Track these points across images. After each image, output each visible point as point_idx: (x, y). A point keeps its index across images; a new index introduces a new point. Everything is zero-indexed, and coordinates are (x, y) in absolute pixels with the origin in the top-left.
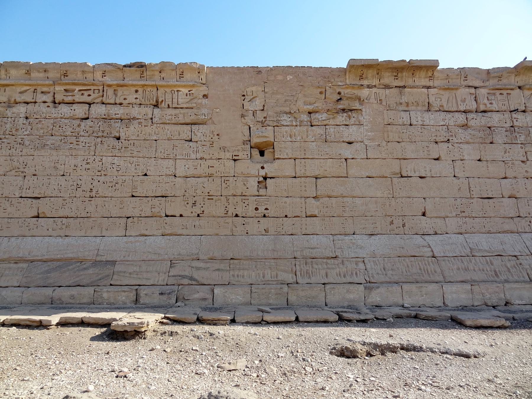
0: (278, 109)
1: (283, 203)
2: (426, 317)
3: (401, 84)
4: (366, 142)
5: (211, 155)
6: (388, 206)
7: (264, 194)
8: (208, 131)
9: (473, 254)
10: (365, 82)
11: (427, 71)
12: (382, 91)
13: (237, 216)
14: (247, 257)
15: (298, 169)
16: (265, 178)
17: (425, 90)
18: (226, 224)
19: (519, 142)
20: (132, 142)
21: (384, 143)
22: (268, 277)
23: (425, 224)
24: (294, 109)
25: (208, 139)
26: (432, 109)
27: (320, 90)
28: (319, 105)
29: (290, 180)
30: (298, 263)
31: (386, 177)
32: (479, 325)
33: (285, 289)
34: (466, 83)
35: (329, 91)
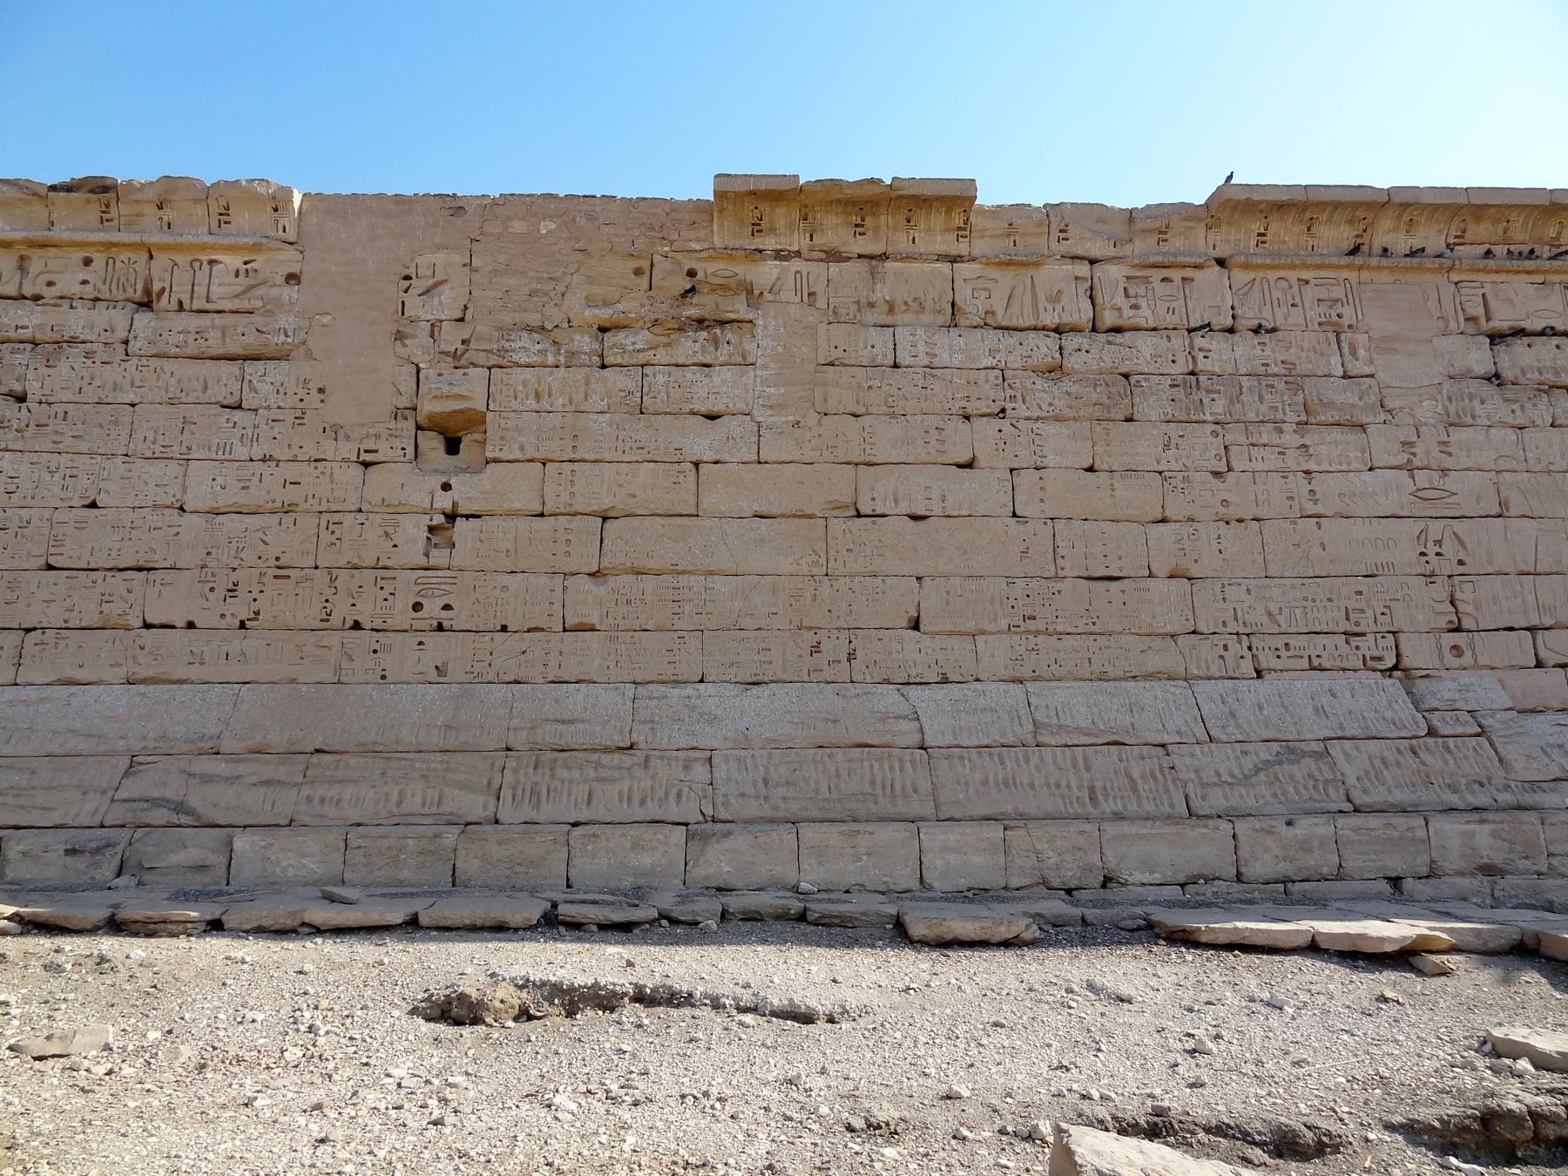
0: (506, 318)
1: (498, 591)
2: (823, 916)
3: (876, 249)
4: (759, 415)
5: (295, 450)
6: (809, 600)
7: (443, 562)
8: (293, 381)
9: (1040, 739)
10: (769, 243)
11: (949, 211)
12: (818, 269)
13: (357, 626)
14: (365, 744)
15: (549, 491)
16: (451, 517)
17: (945, 267)
18: (322, 651)
19: (1209, 418)
20: (60, 409)
21: (812, 419)
22: (413, 803)
23: (916, 652)
24: (555, 316)
25: (291, 401)
26: (963, 322)
27: (634, 264)
28: (630, 307)
29: (523, 524)
30: (511, 764)
31: (811, 517)
32: (949, 936)
33: (451, 836)
34: (1064, 247)
35: (662, 267)
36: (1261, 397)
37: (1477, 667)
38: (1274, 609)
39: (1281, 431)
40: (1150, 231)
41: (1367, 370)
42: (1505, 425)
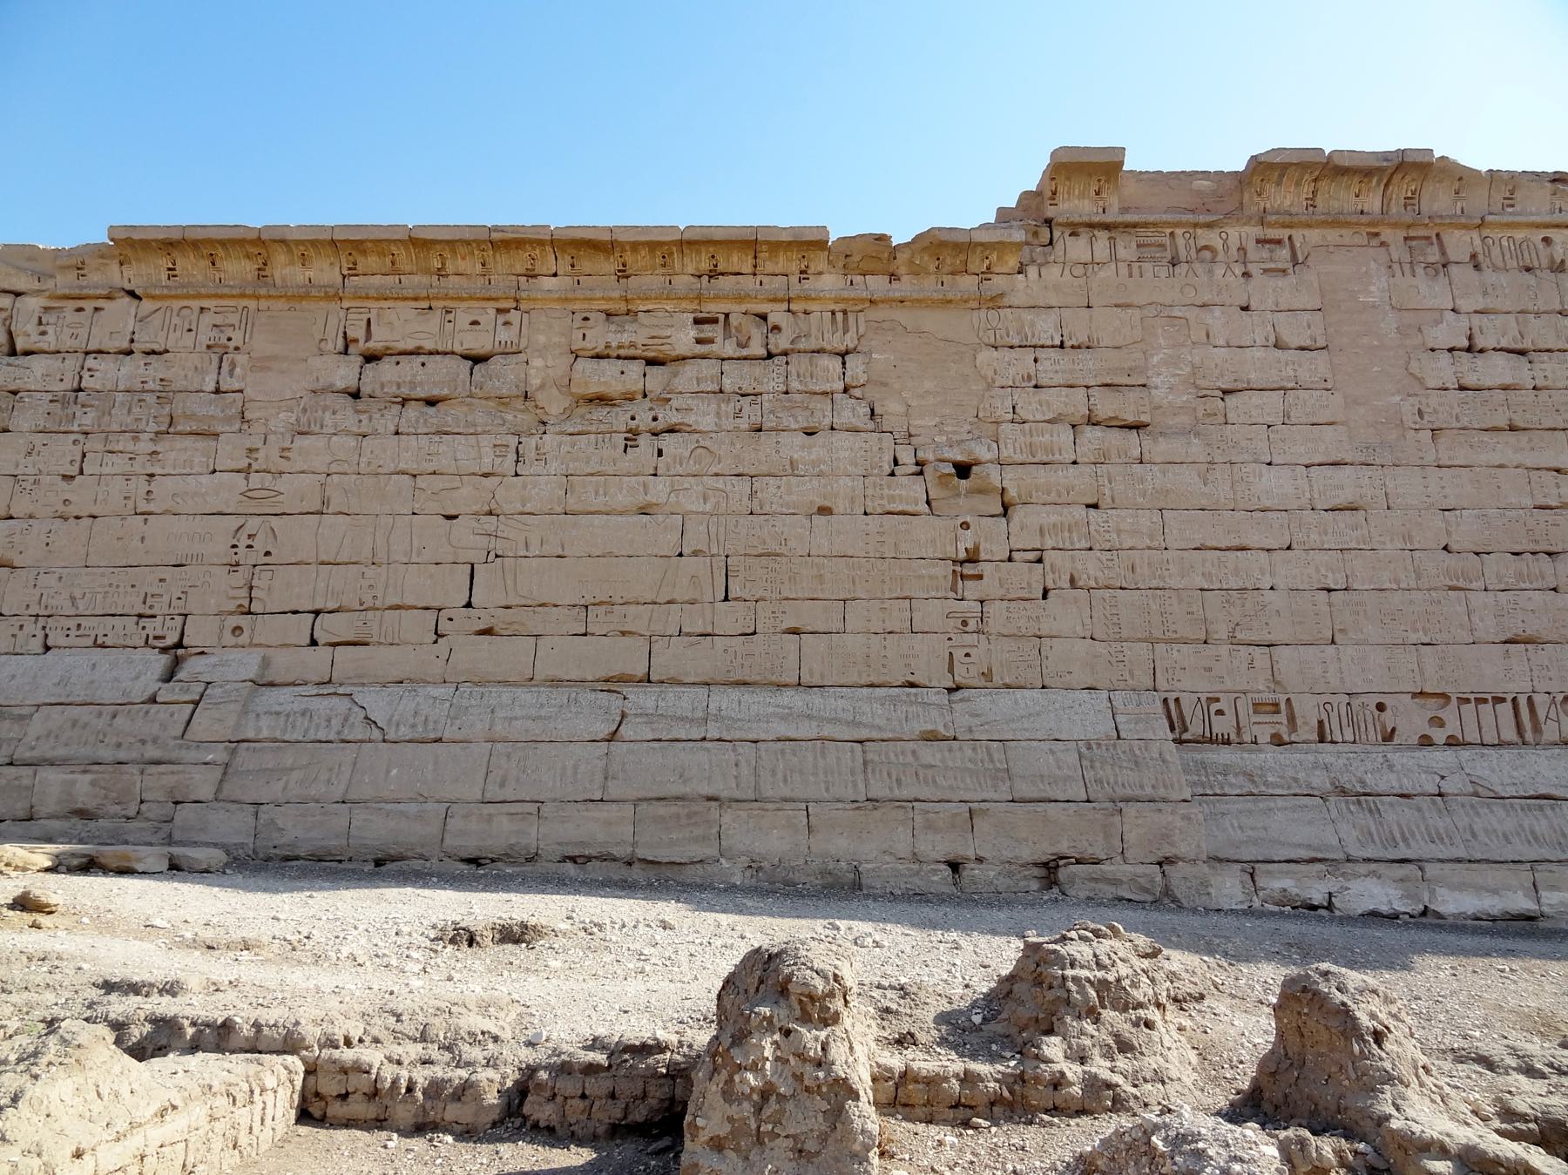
19: (76, 428)
36: (129, 411)
37: (251, 645)
38: (78, 594)
39: (136, 439)
40: (69, 267)
41: (237, 386)
42: (348, 433)
